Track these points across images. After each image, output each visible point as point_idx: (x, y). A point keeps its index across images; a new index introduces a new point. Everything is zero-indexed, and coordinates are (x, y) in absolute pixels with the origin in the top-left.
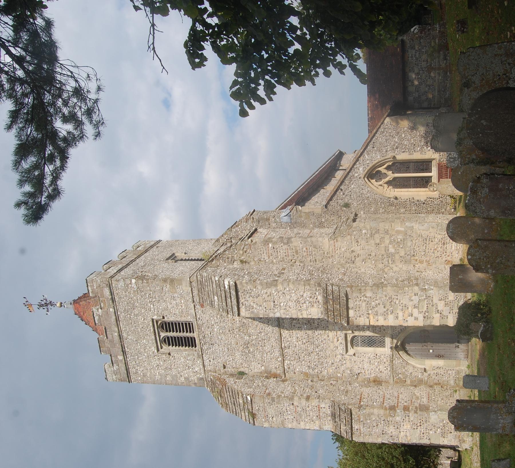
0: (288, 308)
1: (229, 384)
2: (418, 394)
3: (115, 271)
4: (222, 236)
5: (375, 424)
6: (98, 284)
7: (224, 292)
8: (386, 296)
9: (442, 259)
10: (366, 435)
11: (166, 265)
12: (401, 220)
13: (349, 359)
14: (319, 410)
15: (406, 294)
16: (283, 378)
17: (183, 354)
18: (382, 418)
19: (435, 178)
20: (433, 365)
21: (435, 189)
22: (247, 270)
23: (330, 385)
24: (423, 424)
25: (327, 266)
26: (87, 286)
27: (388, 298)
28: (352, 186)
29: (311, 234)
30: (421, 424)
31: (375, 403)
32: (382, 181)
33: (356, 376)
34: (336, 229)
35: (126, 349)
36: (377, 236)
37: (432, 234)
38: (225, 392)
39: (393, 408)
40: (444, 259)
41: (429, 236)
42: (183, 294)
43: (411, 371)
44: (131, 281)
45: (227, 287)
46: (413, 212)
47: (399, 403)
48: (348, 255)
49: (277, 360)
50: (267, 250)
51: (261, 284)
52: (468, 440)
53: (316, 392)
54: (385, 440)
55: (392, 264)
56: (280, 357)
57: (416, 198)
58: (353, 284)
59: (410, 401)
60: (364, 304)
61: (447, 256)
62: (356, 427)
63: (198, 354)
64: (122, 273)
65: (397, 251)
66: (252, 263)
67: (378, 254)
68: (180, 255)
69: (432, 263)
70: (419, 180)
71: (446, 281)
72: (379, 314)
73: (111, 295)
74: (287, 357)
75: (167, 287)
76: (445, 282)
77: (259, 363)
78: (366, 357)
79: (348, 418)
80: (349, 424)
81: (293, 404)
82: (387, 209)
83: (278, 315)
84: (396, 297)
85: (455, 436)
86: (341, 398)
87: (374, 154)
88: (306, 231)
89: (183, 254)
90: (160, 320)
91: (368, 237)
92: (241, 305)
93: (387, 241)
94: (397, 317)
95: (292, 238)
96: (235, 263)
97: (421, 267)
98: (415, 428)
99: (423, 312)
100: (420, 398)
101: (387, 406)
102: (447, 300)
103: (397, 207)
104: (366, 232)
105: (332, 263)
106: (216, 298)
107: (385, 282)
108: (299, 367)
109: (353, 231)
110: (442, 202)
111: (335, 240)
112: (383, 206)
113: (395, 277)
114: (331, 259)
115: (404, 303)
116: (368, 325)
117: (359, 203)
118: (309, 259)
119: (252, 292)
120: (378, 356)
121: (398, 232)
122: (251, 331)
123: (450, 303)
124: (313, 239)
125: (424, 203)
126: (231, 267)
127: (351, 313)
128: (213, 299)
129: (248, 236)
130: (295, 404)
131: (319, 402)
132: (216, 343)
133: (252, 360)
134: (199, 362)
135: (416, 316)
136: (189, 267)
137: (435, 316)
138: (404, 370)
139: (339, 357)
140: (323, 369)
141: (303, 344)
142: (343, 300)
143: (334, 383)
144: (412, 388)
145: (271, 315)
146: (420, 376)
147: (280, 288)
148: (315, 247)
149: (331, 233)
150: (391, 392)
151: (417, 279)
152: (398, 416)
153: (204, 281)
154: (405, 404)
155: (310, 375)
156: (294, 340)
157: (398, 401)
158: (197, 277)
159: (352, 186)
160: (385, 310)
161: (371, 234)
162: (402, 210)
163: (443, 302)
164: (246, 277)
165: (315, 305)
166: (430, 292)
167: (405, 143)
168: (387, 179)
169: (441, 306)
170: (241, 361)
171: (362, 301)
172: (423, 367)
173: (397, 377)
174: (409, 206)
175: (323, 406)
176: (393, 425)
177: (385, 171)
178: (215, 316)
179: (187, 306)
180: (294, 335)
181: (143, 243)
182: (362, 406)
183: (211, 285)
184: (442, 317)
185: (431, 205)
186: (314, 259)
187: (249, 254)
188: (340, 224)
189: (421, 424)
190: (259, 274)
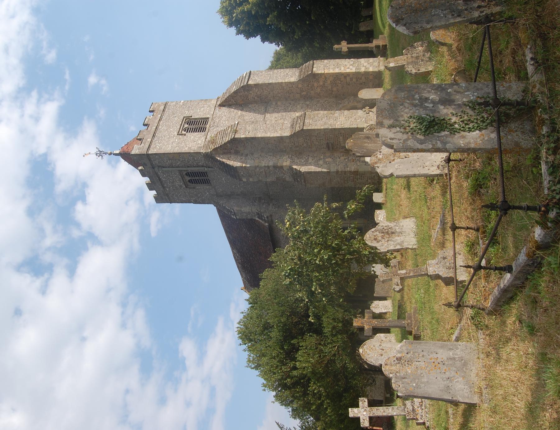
5: (320, 119)
10: (313, 125)
14: (283, 125)
60: (322, 66)
122: (246, 118)
127: (314, 69)
152: (337, 113)
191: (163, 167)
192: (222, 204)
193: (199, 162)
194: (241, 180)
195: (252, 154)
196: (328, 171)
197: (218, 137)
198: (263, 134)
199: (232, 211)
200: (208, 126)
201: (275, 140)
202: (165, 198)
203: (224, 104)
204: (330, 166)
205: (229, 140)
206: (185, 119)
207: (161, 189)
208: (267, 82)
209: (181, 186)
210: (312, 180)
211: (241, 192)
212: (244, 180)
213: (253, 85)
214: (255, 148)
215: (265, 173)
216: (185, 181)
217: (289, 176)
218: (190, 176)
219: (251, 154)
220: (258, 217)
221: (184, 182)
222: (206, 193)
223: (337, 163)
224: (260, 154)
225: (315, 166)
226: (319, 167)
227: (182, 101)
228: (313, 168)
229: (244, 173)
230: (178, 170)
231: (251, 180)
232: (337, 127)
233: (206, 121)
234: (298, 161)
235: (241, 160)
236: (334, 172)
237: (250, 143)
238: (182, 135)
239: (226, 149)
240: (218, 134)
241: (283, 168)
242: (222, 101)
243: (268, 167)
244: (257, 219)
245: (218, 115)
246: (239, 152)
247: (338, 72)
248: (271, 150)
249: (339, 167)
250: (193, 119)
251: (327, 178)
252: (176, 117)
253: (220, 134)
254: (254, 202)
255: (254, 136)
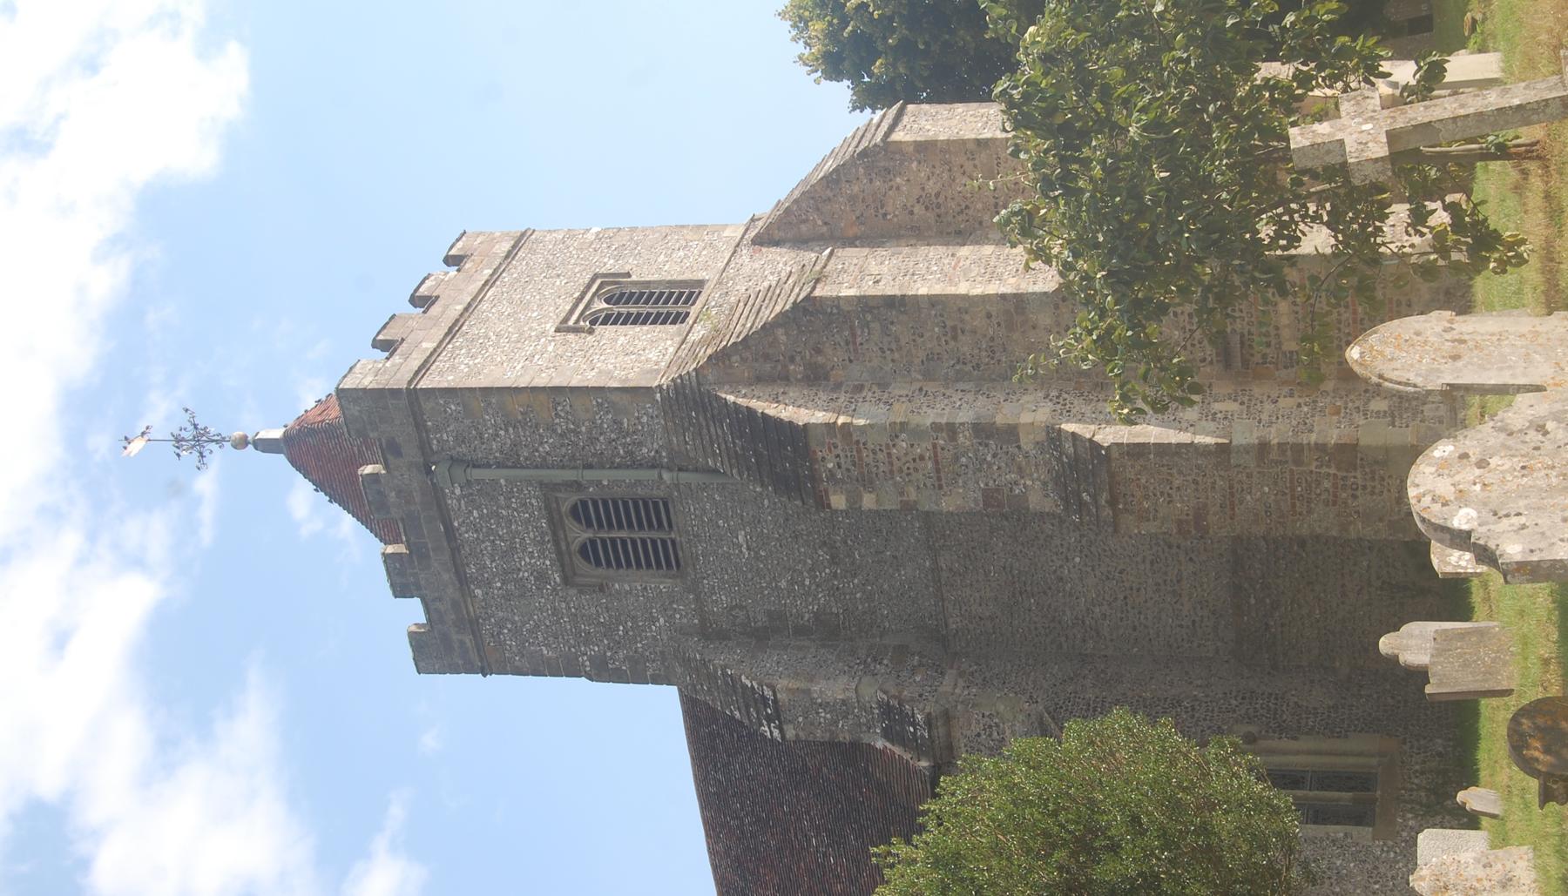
26: (458, 240)
35: (464, 328)
73: (514, 247)
81: (953, 255)
92: (900, 126)
191: (474, 466)
192: (724, 668)
193: (640, 444)
194: (822, 503)
195: (883, 386)
196: (1220, 441)
197: (737, 315)
198: (937, 287)
199: (763, 697)
200: (694, 311)
201: (989, 316)
202: (462, 643)
203: (778, 235)
204: (1230, 426)
205: (787, 307)
206: (598, 282)
207: (450, 590)
208: (973, 136)
209: (542, 577)
210: (1146, 497)
211: (817, 615)
212: (838, 501)
213: (911, 148)
214: (896, 356)
215: (937, 462)
216: (564, 548)
217: (1045, 484)
218: (589, 524)
219: (879, 385)
220: (887, 734)
221: (559, 553)
222: (654, 620)
223: (1265, 417)
224: (917, 386)
225: (1162, 424)
226: (1181, 430)
227: (595, 230)
228: (1151, 432)
229: (840, 467)
230: (541, 484)
231: (868, 501)
233: (691, 294)
234: (1087, 409)
235: (832, 405)
236: (1247, 449)
237: (875, 326)
238: (576, 330)
239: (767, 357)
240: (741, 304)
241: (1018, 440)
242: (770, 220)
243: (951, 430)
244: (880, 744)
245: (746, 270)
246: (827, 378)
248: (968, 368)
249: (1273, 430)
250: (635, 283)
251: (1214, 483)
252: (559, 276)
253: (750, 303)
254: (875, 660)
255: (898, 293)
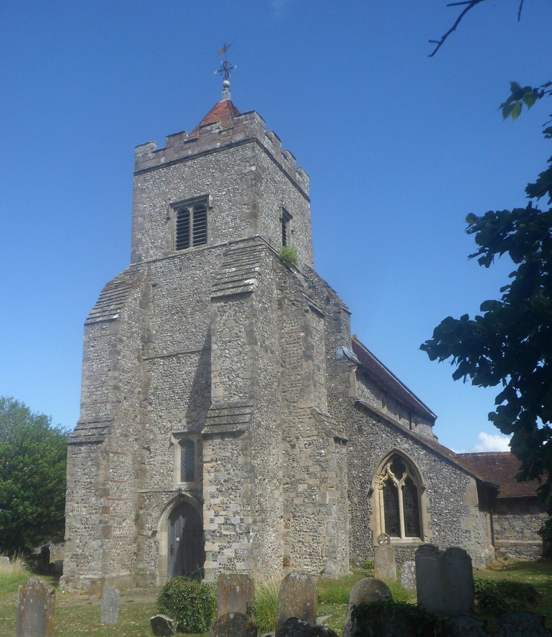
0: (222, 359)
1: (133, 292)
2: (124, 524)
3: (266, 146)
4: (317, 276)
6: (249, 125)
7: (240, 278)
8: (239, 482)
9: (292, 552)
11: (276, 208)
12: (340, 499)
13: (167, 436)
14: (103, 403)
15: (242, 508)
16: (143, 357)
17: (169, 235)
18: (93, 480)
19: (399, 542)
20: (160, 542)
21: (381, 542)
22: (271, 306)
23: (135, 415)
24: (88, 531)
25: (278, 406)
27: (236, 484)
28: (384, 435)
29: (319, 385)
30: (87, 529)
31: (111, 470)
32: (392, 473)
33: (146, 446)
34: (326, 416)
36: (318, 468)
37: (322, 539)
38: (123, 288)
39: (105, 493)
40: (291, 555)
41: (319, 535)
42: (240, 230)
43: (153, 514)
44: (254, 165)
45: (246, 282)
46: (354, 513)
47: (112, 501)
48: (294, 432)
49: (164, 348)
50: (296, 330)
51: (251, 324)
52: (69, 587)
53: (125, 398)
54: (70, 485)
55: (284, 488)
56: (167, 352)
57: (371, 517)
58: (253, 439)
59: (115, 514)
60: (229, 454)
61: (295, 558)
62: (82, 448)
63: (169, 253)
64: (263, 155)
65: (299, 495)
66: (279, 313)
67: (296, 471)
68: (291, 224)
69: (286, 539)
70: (395, 521)
71: (261, 559)
72: (216, 473)
74: (168, 361)
75: (246, 210)
76: (259, 557)
77: (159, 327)
78: (169, 458)
79: (93, 438)
80: (86, 439)
81: (109, 370)
82: (356, 480)
83: (214, 347)
84: (238, 495)
85: (73, 572)
86: (118, 428)
87: (426, 462)
88: (323, 378)
89: (291, 229)
90: (208, 204)
91: (316, 457)
93: (311, 482)
94: (213, 497)
95: (313, 360)
96: (279, 292)
97: (281, 526)
98: (83, 522)
99: (221, 529)
100: (120, 526)
101: (108, 486)
102: (236, 561)
103: (360, 493)
104: (322, 455)
105: (283, 413)
106: (234, 269)
107: (257, 481)
108: (155, 376)
109: (323, 439)
110: (368, 551)
111: (310, 416)
112: (360, 475)
113: (265, 494)
114: (287, 411)
115: (231, 505)
116: (204, 460)
117: (363, 444)
118: (286, 383)
119: (240, 314)
120: (170, 472)
121: (324, 496)
123: (233, 565)
124: (312, 387)
125: (366, 527)
126: (273, 287)
128: (232, 266)
129: (314, 306)
130: (110, 372)
131: (113, 402)
132: (182, 273)
133: (163, 319)
134: (160, 255)
135: (215, 520)
136: (275, 235)
137: (217, 544)
138: (154, 506)
139: (169, 425)
140: (154, 405)
141: (183, 379)
142: (233, 428)
143: (138, 420)
144: (133, 516)
145: (214, 339)
146: (147, 525)
147: (247, 348)
148: (302, 390)
149: (321, 410)
150: (127, 490)
151: (263, 521)
152: (97, 500)
153: (255, 254)
154: (111, 508)
155: (147, 390)
156: (187, 369)
157: (115, 499)
158: (260, 245)
159: (384, 435)
160: (222, 481)
161: (321, 461)
162: (356, 500)
163: (233, 555)
164: (260, 305)
165: (227, 393)
166: (246, 538)
167: (442, 502)
168: (395, 479)
169: (229, 553)
170: (162, 305)
171: (232, 452)
172: (158, 529)
173: (146, 498)
174: (361, 508)
175: (109, 406)
176: (85, 494)
177: (405, 476)
178: (214, 270)
179: (225, 236)
180: (193, 369)
181: (305, 180)
182: (108, 454)
183: (250, 262)
184: (215, 555)
185: (363, 536)
186: (286, 389)
187: (290, 308)
188: (333, 421)
189: (87, 529)
190: (264, 322)
232: (69, 506)
247: (204, 491)
